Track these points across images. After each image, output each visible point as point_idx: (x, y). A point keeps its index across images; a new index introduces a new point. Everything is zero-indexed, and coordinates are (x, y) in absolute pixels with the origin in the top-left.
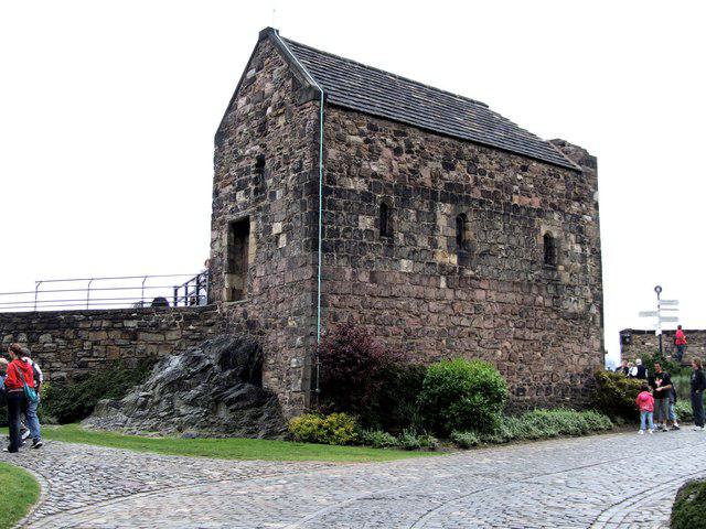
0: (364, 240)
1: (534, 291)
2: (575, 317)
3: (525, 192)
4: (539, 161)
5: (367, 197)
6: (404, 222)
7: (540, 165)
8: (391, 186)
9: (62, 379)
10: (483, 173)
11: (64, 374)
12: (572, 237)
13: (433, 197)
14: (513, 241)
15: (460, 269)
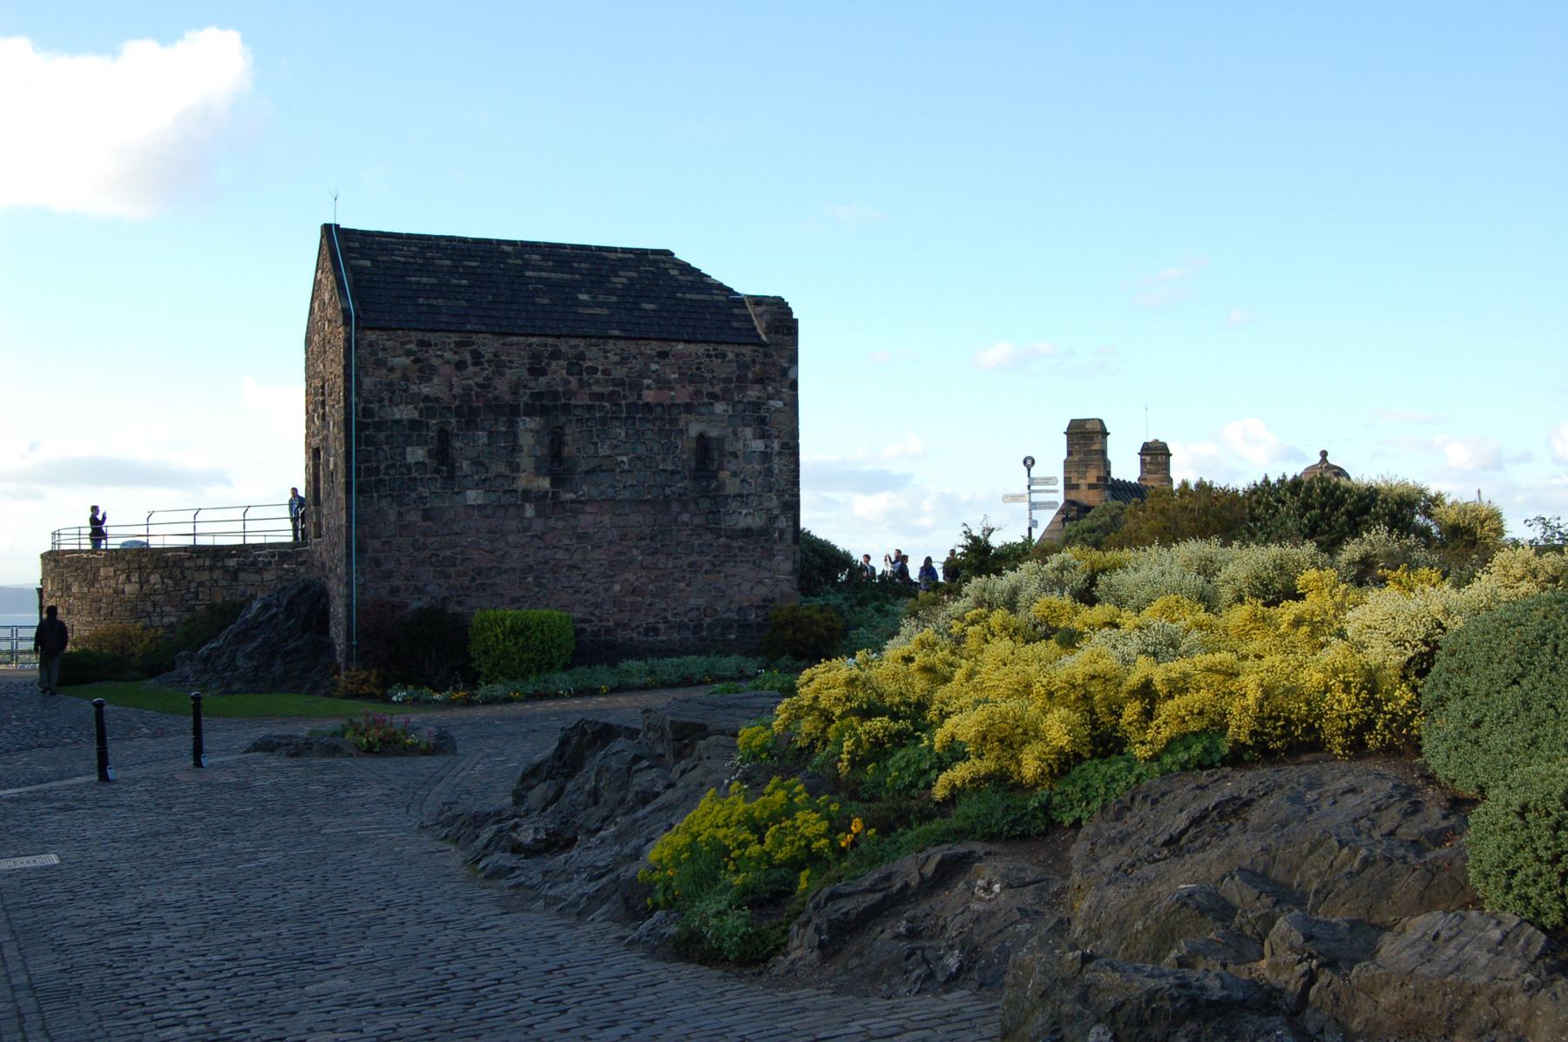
0: (414, 475)
1: (675, 507)
2: (747, 533)
3: (663, 384)
5: (415, 425)
6: (469, 448)
7: (692, 347)
8: (449, 408)
9: (172, 624)
10: (594, 370)
11: (174, 619)
12: (748, 432)
13: (514, 412)
14: (641, 450)
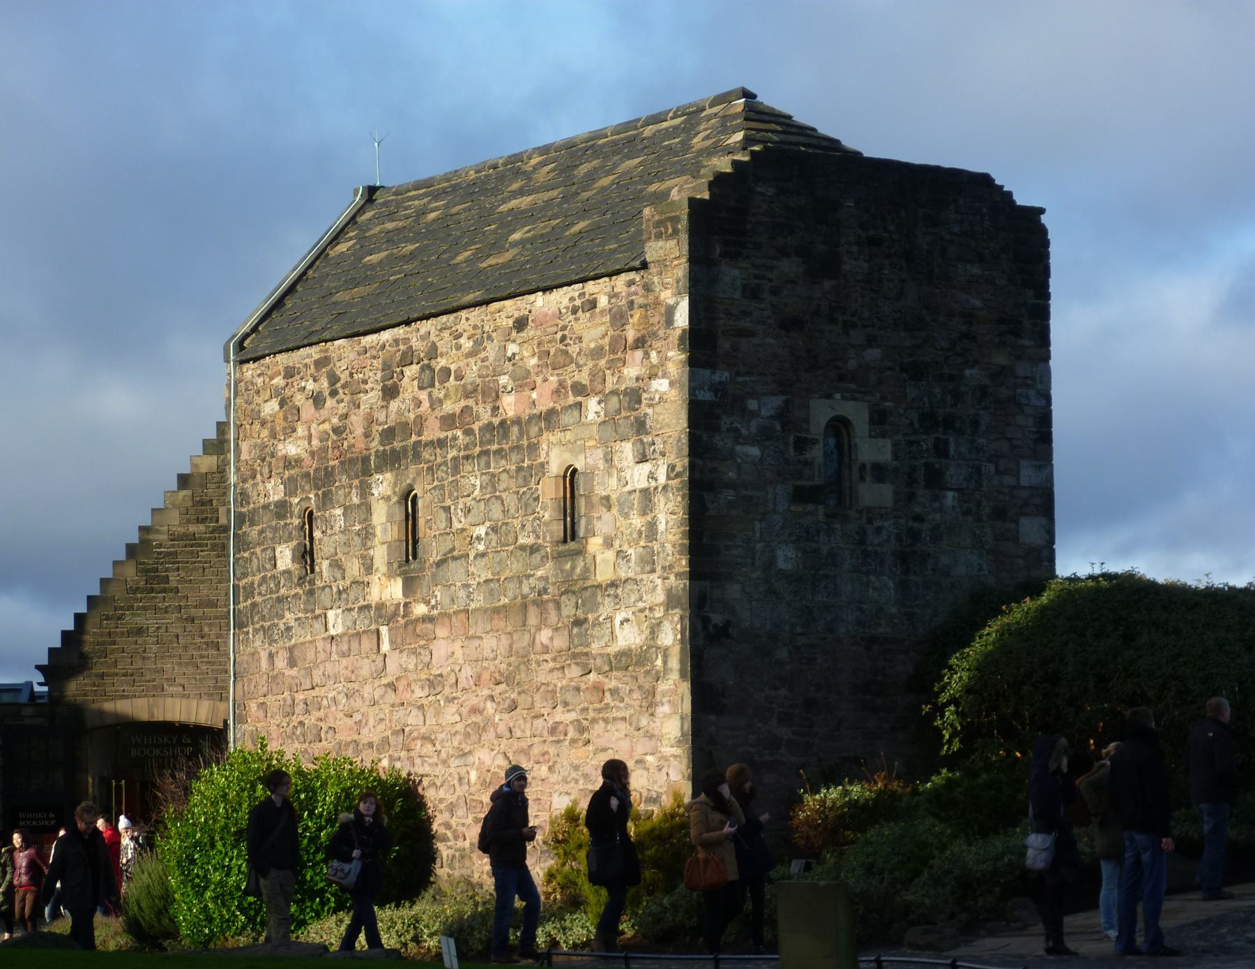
0: (283, 591)
1: (533, 620)
3: (523, 382)
4: (546, 289)
15: (406, 605)
